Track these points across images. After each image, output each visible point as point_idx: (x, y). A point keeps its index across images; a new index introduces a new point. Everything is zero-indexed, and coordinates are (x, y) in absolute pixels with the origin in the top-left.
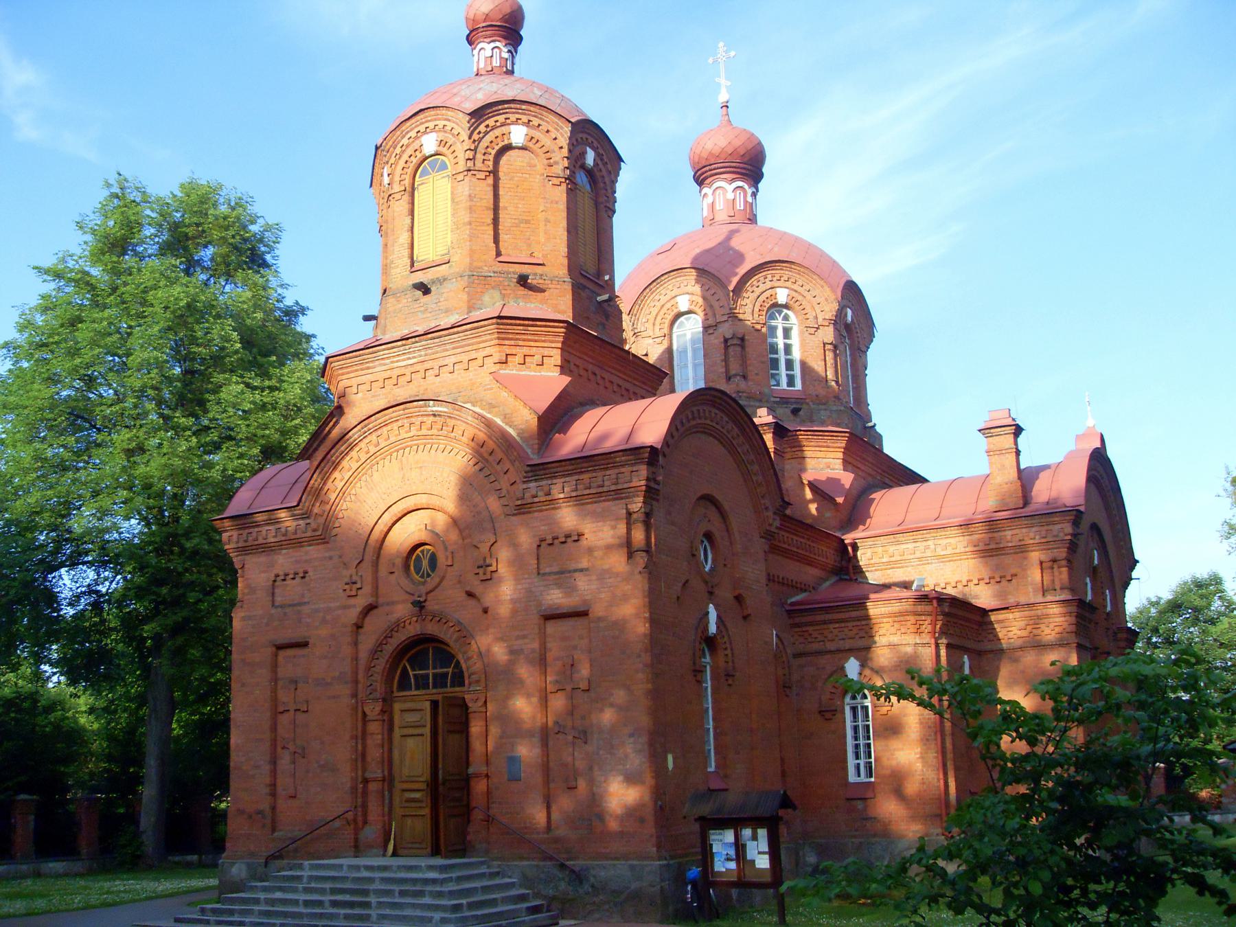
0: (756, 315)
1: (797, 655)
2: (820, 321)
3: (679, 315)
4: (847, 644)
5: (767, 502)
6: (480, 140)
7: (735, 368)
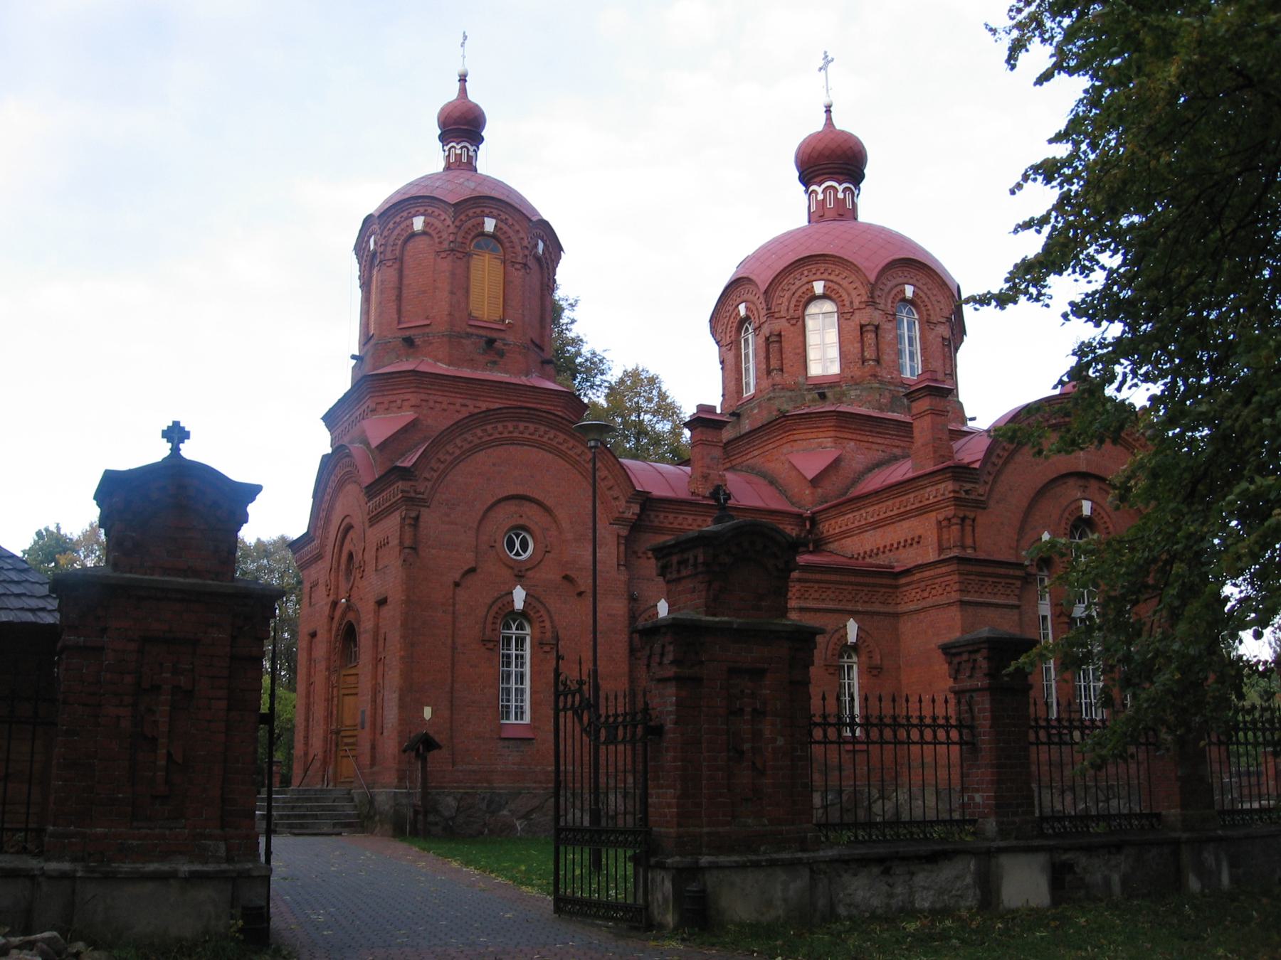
0: (791, 311)
2: (856, 304)
5: (615, 493)
6: (389, 235)
7: (774, 363)
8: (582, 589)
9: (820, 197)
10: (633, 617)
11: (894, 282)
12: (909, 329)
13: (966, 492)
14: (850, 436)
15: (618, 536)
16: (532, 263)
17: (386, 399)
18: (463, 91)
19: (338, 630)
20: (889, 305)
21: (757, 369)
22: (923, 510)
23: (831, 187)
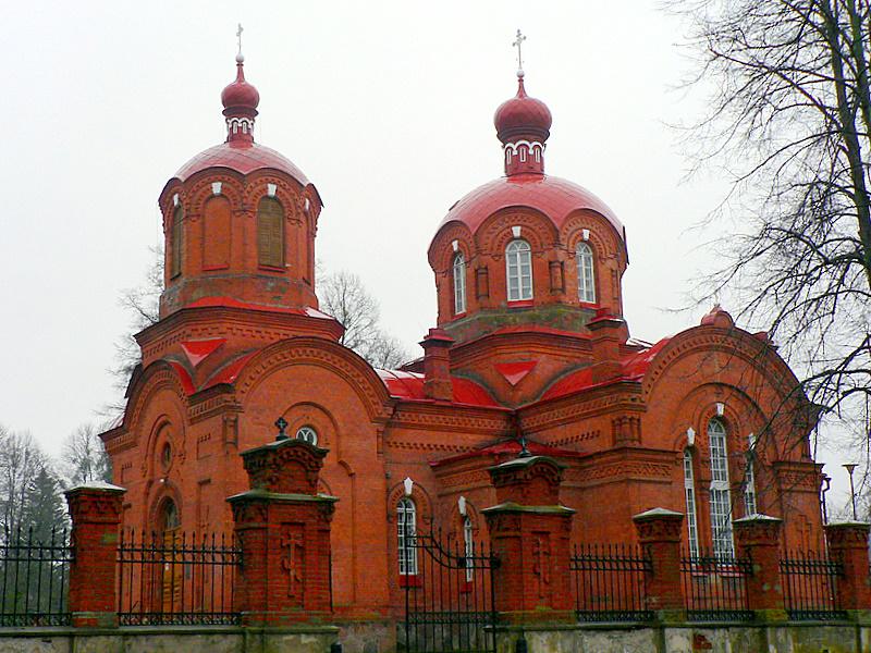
1: (440, 496)
3: (455, 254)
4: (461, 488)
8: (353, 471)
9: (515, 153)
10: (388, 491)
11: (574, 227)
12: (584, 265)
13: (633, 400)
14: (543, 350)
15: (378, 431)
16: (303, 219)
17: (199, 327)
18: (240, 74)
19: (154, 503)
20: (571, 245)
21: (468, 295)
22: (599, 413)
23: (524, 145)
